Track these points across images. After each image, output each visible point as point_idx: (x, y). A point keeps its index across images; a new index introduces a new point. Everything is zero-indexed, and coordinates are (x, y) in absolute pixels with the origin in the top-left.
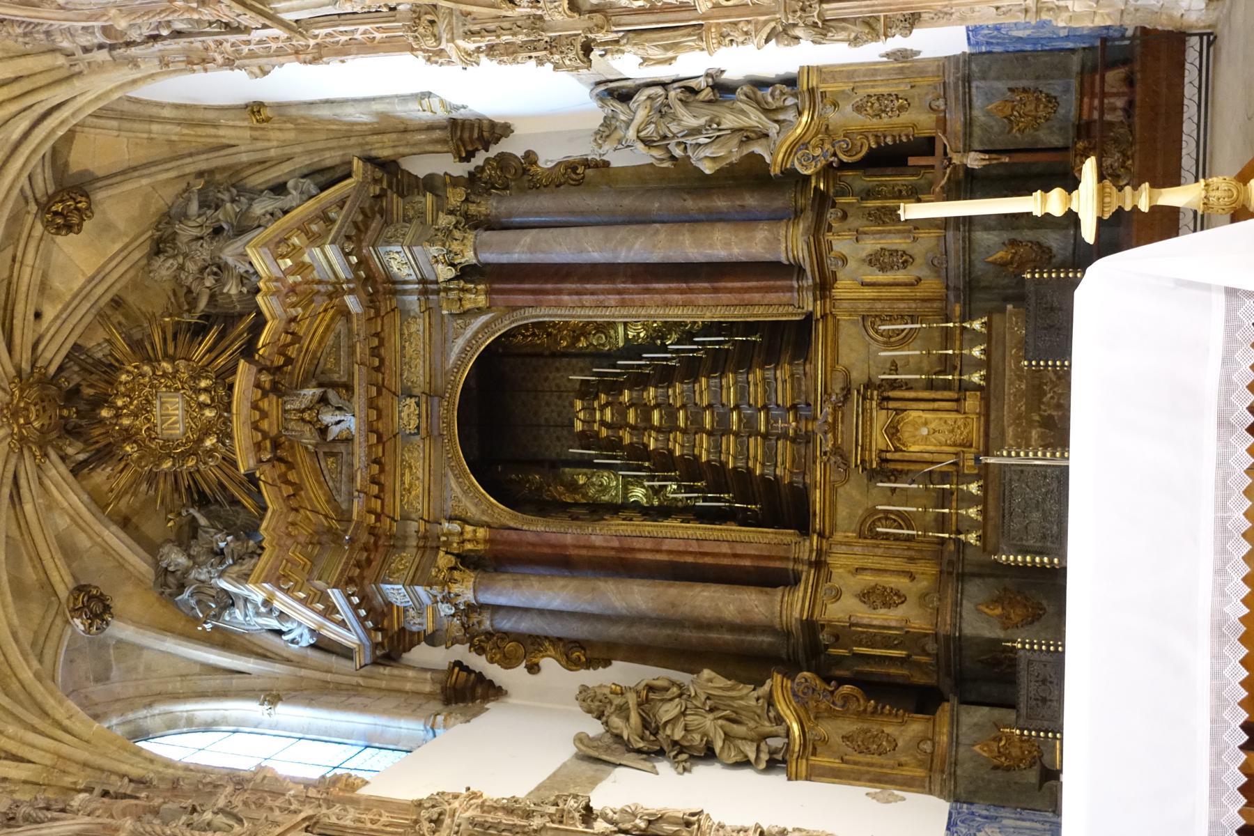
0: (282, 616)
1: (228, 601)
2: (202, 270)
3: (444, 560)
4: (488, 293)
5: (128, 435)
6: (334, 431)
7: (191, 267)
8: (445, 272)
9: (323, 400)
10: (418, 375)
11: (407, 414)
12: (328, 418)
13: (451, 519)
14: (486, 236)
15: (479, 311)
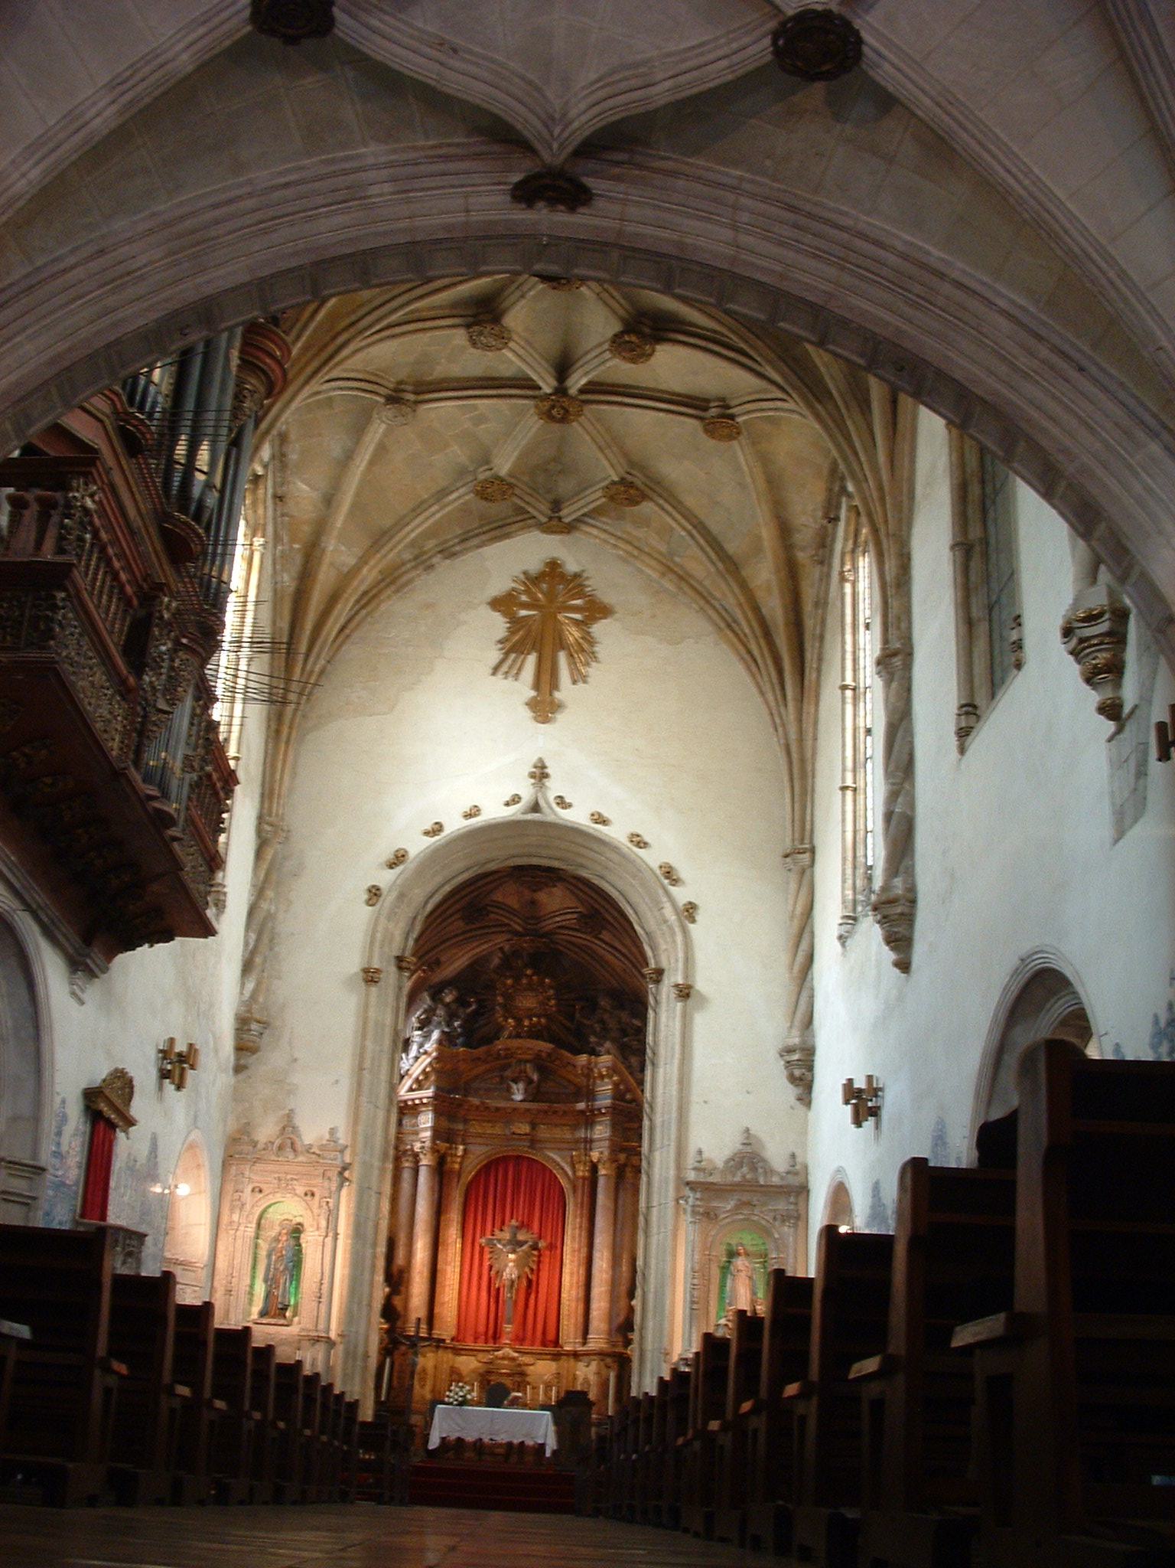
0: (417, 1058)
1: (423, 1025)
2: (602, 1021)
3: (443, 1146)
4: (584, 1178)
5: (517, 979)
6: (514, 1086)
7: (606, 1016)
8: (595, 1155)
9: (530, 1081)
10: (543, 1132)
11: (525, 1128)
12: (521, 1086)
13: (465, 1150)
14: (613, 1180)
15: (574, 1172)
